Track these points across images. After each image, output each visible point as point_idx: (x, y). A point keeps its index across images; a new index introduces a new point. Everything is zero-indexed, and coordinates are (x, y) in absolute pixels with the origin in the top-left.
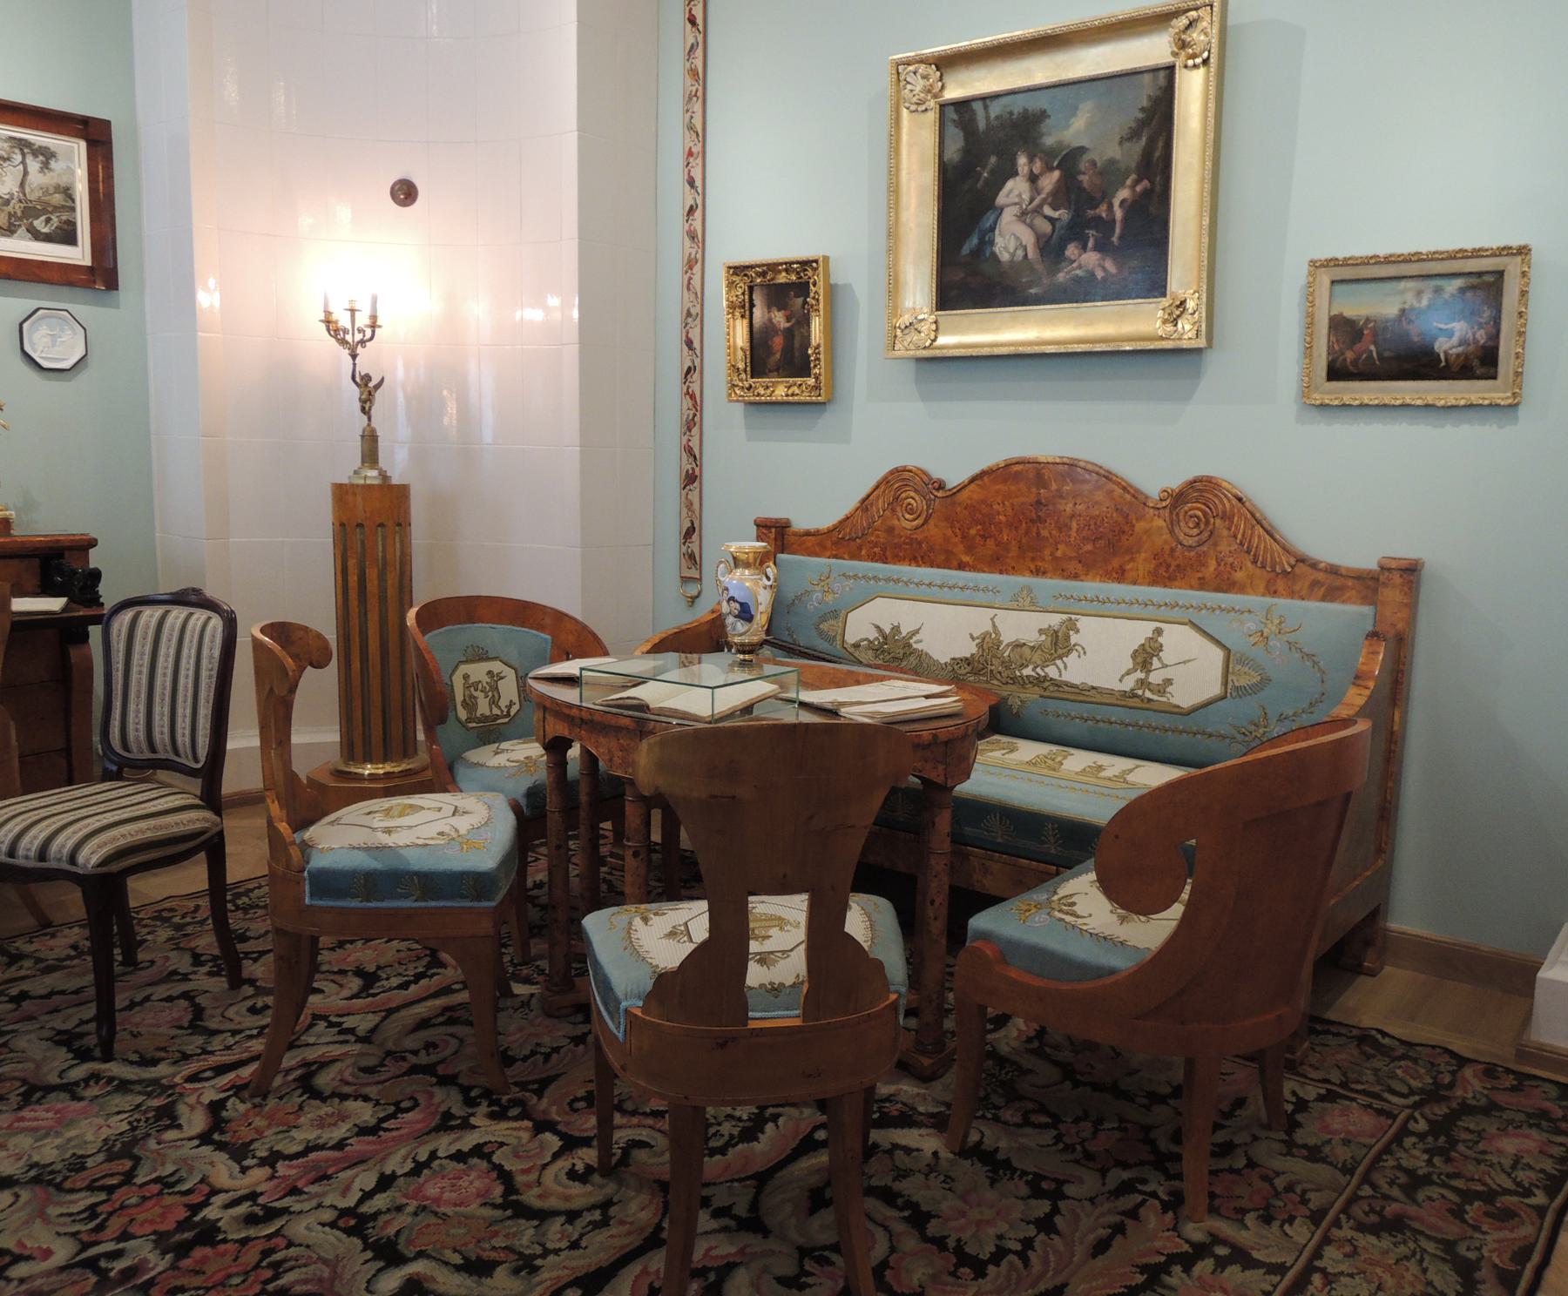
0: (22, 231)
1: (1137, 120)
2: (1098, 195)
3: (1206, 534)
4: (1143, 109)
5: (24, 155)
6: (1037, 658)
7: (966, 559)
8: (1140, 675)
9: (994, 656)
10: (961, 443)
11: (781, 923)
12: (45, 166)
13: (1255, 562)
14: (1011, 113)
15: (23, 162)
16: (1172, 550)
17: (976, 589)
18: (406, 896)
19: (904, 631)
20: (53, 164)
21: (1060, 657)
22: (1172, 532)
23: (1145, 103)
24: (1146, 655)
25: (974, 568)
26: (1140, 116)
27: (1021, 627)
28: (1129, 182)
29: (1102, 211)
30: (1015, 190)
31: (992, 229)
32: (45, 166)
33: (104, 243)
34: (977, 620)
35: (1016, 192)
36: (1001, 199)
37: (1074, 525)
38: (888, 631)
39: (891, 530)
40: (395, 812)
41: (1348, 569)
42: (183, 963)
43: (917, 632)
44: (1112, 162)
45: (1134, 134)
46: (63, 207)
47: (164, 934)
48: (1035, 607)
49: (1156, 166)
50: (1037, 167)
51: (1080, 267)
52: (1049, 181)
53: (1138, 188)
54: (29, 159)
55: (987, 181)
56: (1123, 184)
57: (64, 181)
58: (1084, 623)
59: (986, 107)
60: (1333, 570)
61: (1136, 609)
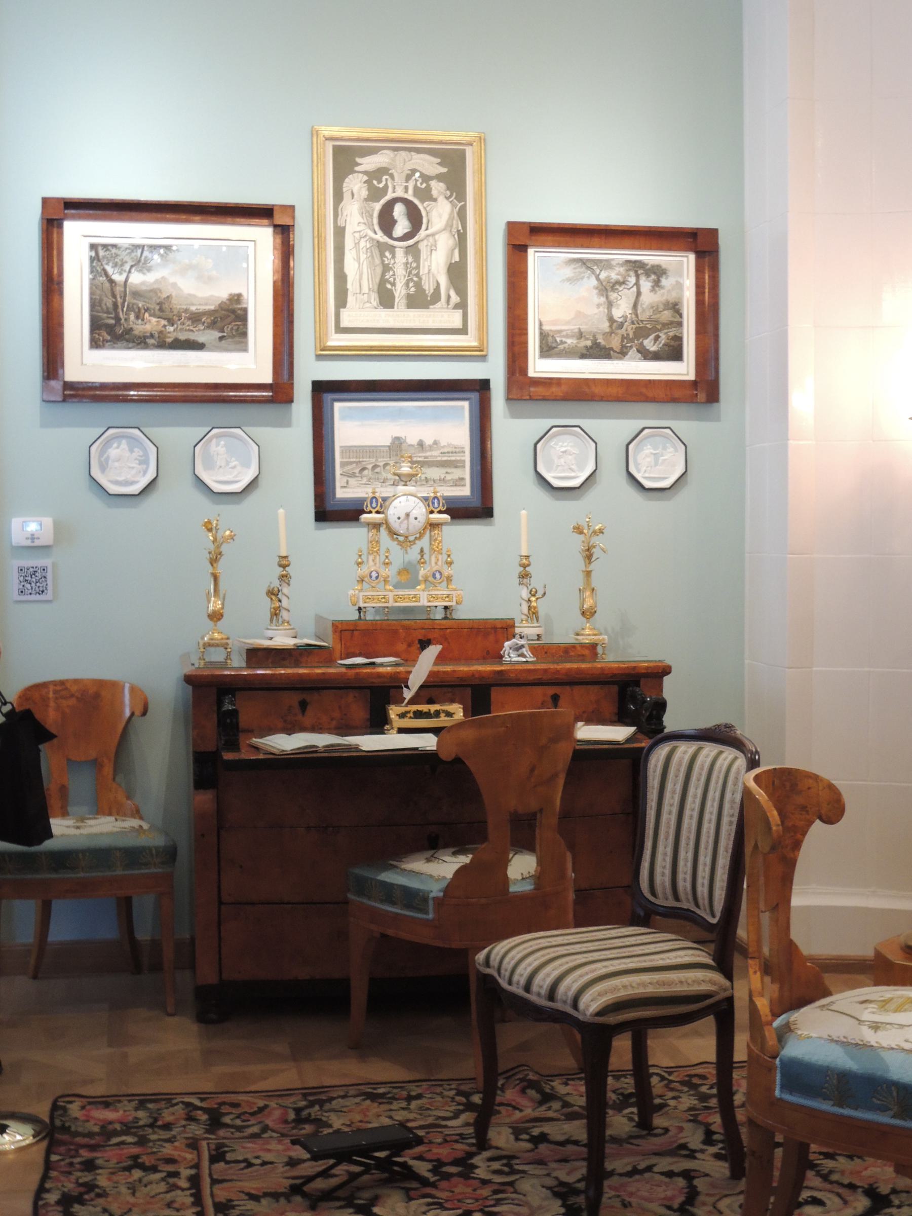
0: (633, 352)
5: (637, 276)
12: (657, 284)
15: (637, 284)
18: (883, 1109)
20: (664, 282)
32: (657, 284)
40: (892, 1006)
42: (694, 1139)
46: (672, 323)
47: (688, 1101)
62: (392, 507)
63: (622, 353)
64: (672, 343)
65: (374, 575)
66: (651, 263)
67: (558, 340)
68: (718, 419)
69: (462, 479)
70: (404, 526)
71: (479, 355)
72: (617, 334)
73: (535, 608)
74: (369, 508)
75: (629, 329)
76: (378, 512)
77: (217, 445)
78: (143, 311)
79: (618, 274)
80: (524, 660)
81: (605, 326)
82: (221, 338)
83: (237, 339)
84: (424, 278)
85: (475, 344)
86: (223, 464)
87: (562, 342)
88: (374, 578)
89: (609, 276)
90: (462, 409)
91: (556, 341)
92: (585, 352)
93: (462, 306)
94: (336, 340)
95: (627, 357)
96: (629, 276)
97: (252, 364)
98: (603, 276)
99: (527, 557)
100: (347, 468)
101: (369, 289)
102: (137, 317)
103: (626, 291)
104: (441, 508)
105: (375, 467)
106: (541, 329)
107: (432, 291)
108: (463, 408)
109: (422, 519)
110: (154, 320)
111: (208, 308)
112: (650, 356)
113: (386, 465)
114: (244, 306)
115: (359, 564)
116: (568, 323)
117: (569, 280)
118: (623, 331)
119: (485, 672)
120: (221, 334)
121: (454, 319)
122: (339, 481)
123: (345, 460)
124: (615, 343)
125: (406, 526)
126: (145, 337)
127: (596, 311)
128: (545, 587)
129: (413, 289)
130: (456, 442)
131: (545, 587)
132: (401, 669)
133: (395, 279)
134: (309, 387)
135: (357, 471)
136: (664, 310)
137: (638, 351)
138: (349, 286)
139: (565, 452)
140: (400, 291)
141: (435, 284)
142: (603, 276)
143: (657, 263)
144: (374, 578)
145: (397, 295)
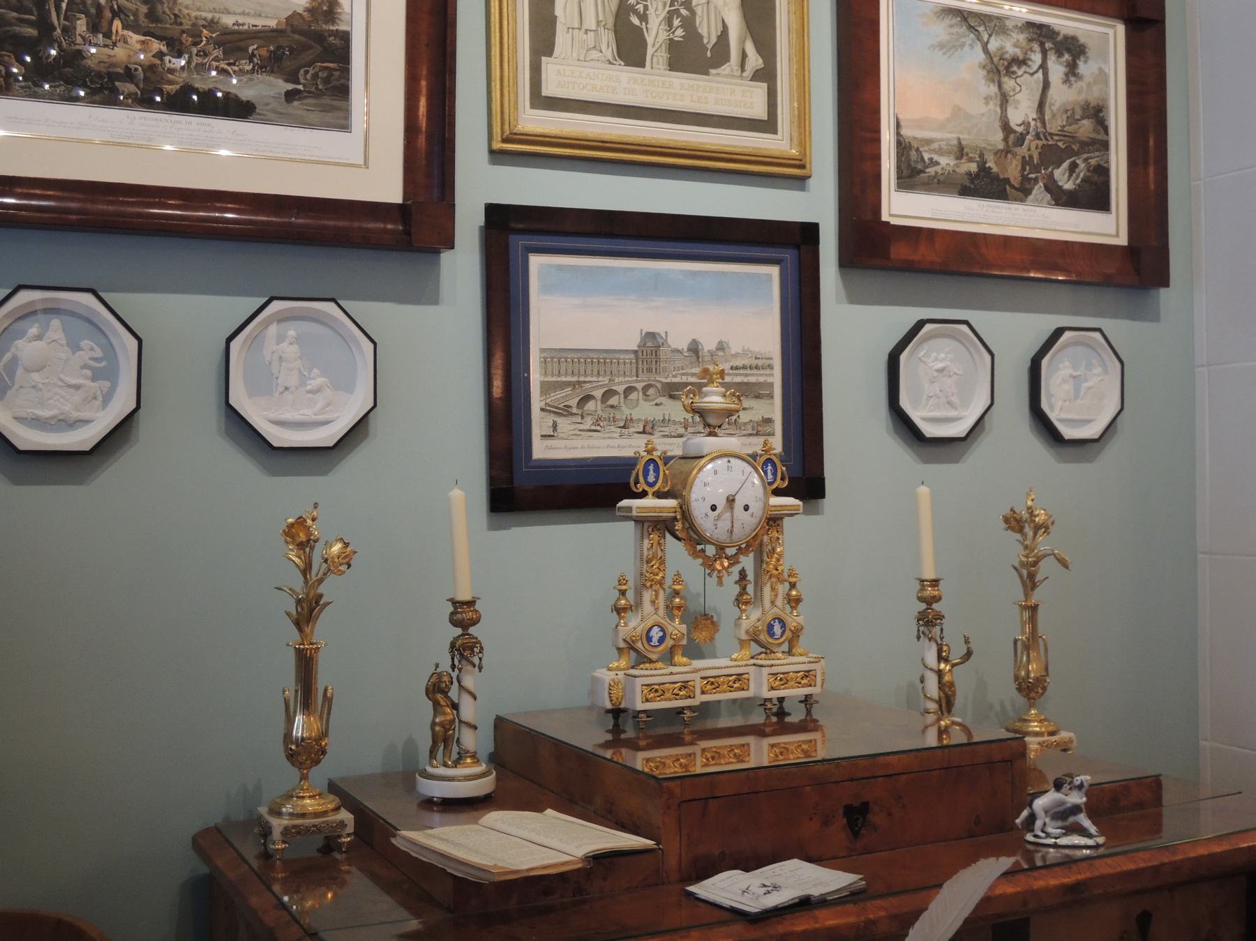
0: (1038, 190)
15: (1043, 66)
20: (1082, 68)
33: (1150, 211)
54: (1052, 58)
57: (1093, 96)
62: (698, 484)
63: (1022, 192)
64: (1095, 178)
65: (656, 634)
66: (1064, 32)
67: (926, 156)
68: (1153, 316)
69: (769, 421)
70: (725, 524)
71: (791, 174)
72: (1015, 155)
73: (952, 685)
74: (642, 486)
75: (1031, 147)
76: (659, 495)
77: (280, 339)
78: (108, 14)
79: (1015, 46)
80: (1090, 842)
81: (997, 138)
82: (290, 96)
83: (326, 100)
84: (699, 11)
85: (794, 152)
86: (293, 381)
87: (933, 163)
88: (655, 641)
89: (1002, 48)
90: (766, 279)
91: (922, 158)
92: (967, 183)
93: (767, 75)
94: (535, 121)
95: (1030, 197)
96: (1031, 50)
97: (359, 159)
98: (994, 45)
99: (935, 583)
100: (556, 397)
101: (598, 23)
102: (94, 28)
103: (1026, 76)
104: (778, 483)
105: (609, 394)
106: (898, 134)
107: (714, 40)
108: (769, 276)
109: (757, 509)
110: (134, 38)
111: (261, 23)
112: (1064, 198)
113: (629, 390)
114: (343, 27)
115: (619, 611)
116: (941, 127)
117: (941, 46)
118: (1022, 151)
119: (1047, 890)
120: (290, 87)
121: (752, 102)
122: (539, 423)
123: (550, 379)
124: (1013, 171)
125: (727, 525)
126: (112, 77)
127: (984, 109)
128: (967, 641)
129: (680, 32)
130: (756, 348)
131: (967, 641)
132: (876, 910)
133: (646, 8)
134: (480, 219)
135: (574, 402)
136: (1083, 118)
137: (1047, 189)
138: (559, 11)
139: (941, 371)
140: (656, 34)
141: (720, 28)
142: (994, 45)
143: (1071, 33)
144: (655, 641)
145: (650, 40)
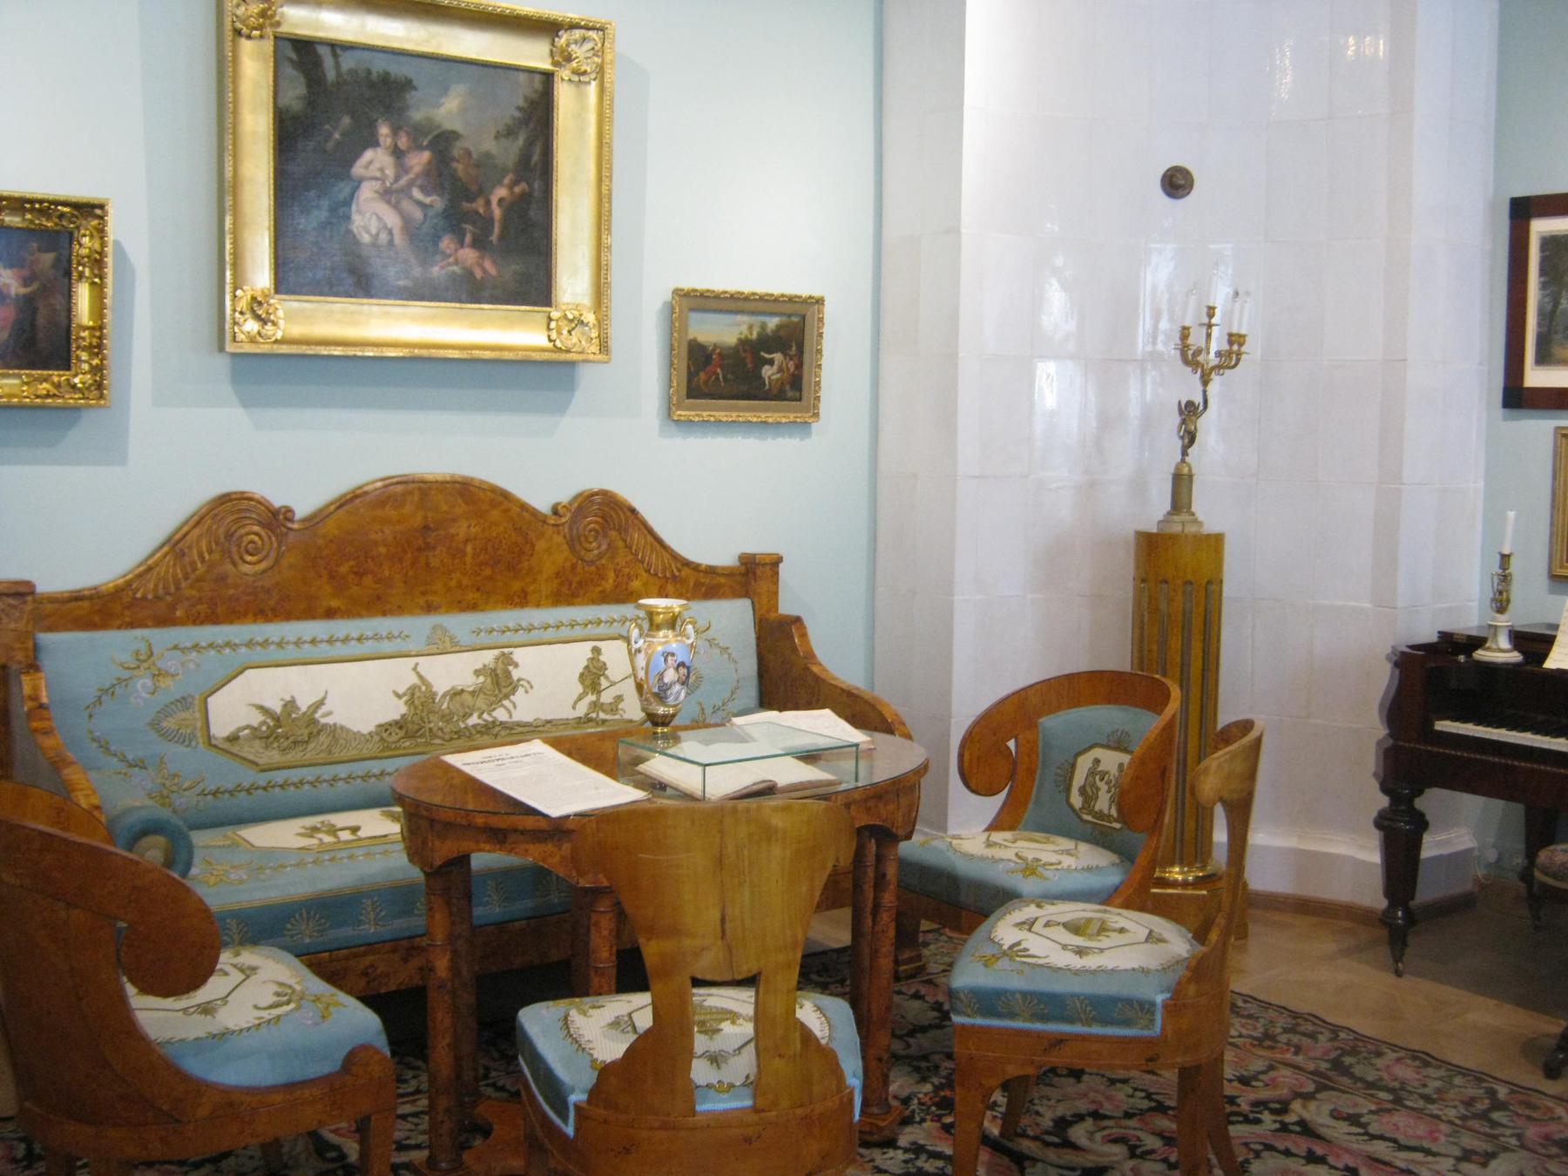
1: (514, 118)
2: (474, 188)
3: (604, 547)
4: (519, 109)
6: (480, 702)
7: (335, 603)
8: (591, 698)
9: (431, 712)
10: (313, 462)
11: (733, 1016)
13: (648, 571)
14: (369, 72)
16: (574, 567)
17: (377, 637)
19: (304, 704)
21: (507, 697)
22: (572, 547)
23: (521, 103)
24: (593, 676)
25: (348, 613)
26: (517, 114)
27: (452, 672)
28: (506, 181)
29: (479, 205)
30: (374, 162)
31: (348, 203)
34: (400, 674)
35: (377, 165)
36: (358, 169)
37: (469, 548)
38: (278, 710)
39: (222, 579)
41: (723, 568)
43: (321, 703)
44: (488, 155)
45: (510, 132)
48: (458, 648)
49: (537, 167)
50: (403, 142)
51: (456, 262)
52: (419, 160)
53: (517, 190)
55: (338, 144)
56: (499, 183)
58: (519, 654)
59: (335, 55)
60: (711, 571)
61: (565, 632)
